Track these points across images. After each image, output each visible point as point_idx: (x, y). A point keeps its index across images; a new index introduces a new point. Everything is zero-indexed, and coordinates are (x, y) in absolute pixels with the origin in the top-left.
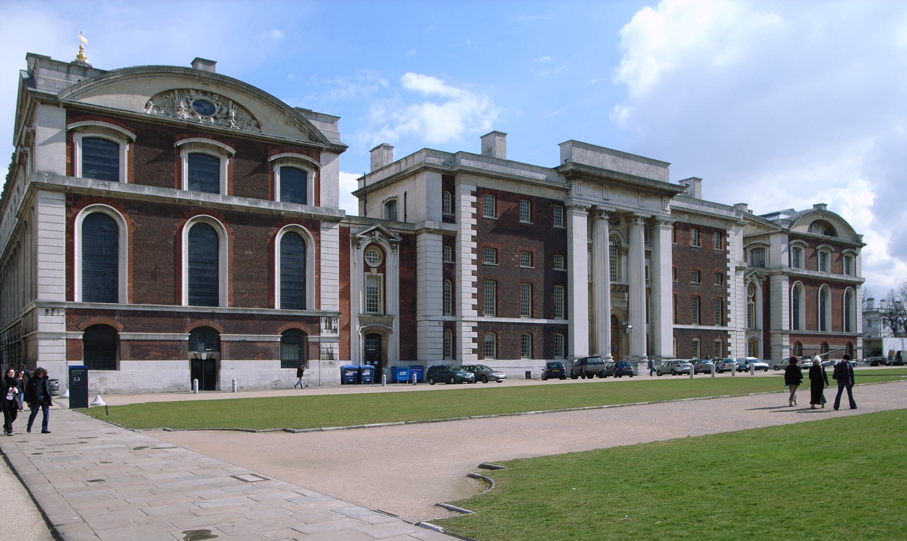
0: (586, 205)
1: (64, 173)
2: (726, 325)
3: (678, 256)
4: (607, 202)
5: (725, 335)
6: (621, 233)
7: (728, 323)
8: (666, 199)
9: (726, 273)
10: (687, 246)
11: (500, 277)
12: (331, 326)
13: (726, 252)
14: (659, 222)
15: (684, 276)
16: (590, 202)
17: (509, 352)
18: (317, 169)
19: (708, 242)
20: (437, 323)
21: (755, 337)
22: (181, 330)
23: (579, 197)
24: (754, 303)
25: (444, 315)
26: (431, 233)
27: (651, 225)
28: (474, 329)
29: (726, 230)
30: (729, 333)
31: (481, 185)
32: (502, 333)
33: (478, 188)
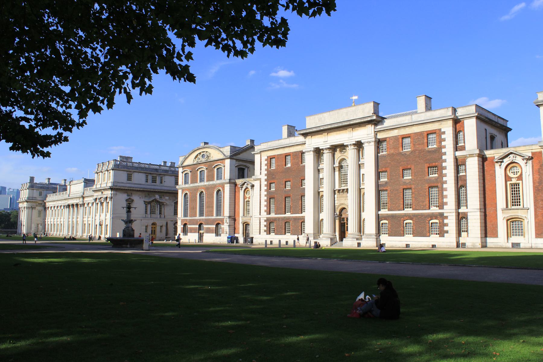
0: (310, 149)
1: (181, 184)
2: (443, 208)
3: (389, 161)
4: (327, 143)
5: (442, 216)
6: (340, 156)
7: (445, 207)
8: (369, 127)
9: (442, 165)
10: (397, 152)
11: (276, 196)
12: (226, 221)
13: (441, 147)
14: (363, 144)
15: (394, 175)
16: (312, 147)
17: (280, 231)
18: (224, 166)
19: (419, 144)
20: (257, 219)
21: (518, 215)
22: (213, 224)
23: (310, 146)
24: (520, 182)
25: (260, 215)
26: (256, 180)
27: (359, 145)
28: (265, 221)
29: (440, 130)
30: (445, 215)
31: (268, 155)
32: (277, 222)
33: (268, 157)
